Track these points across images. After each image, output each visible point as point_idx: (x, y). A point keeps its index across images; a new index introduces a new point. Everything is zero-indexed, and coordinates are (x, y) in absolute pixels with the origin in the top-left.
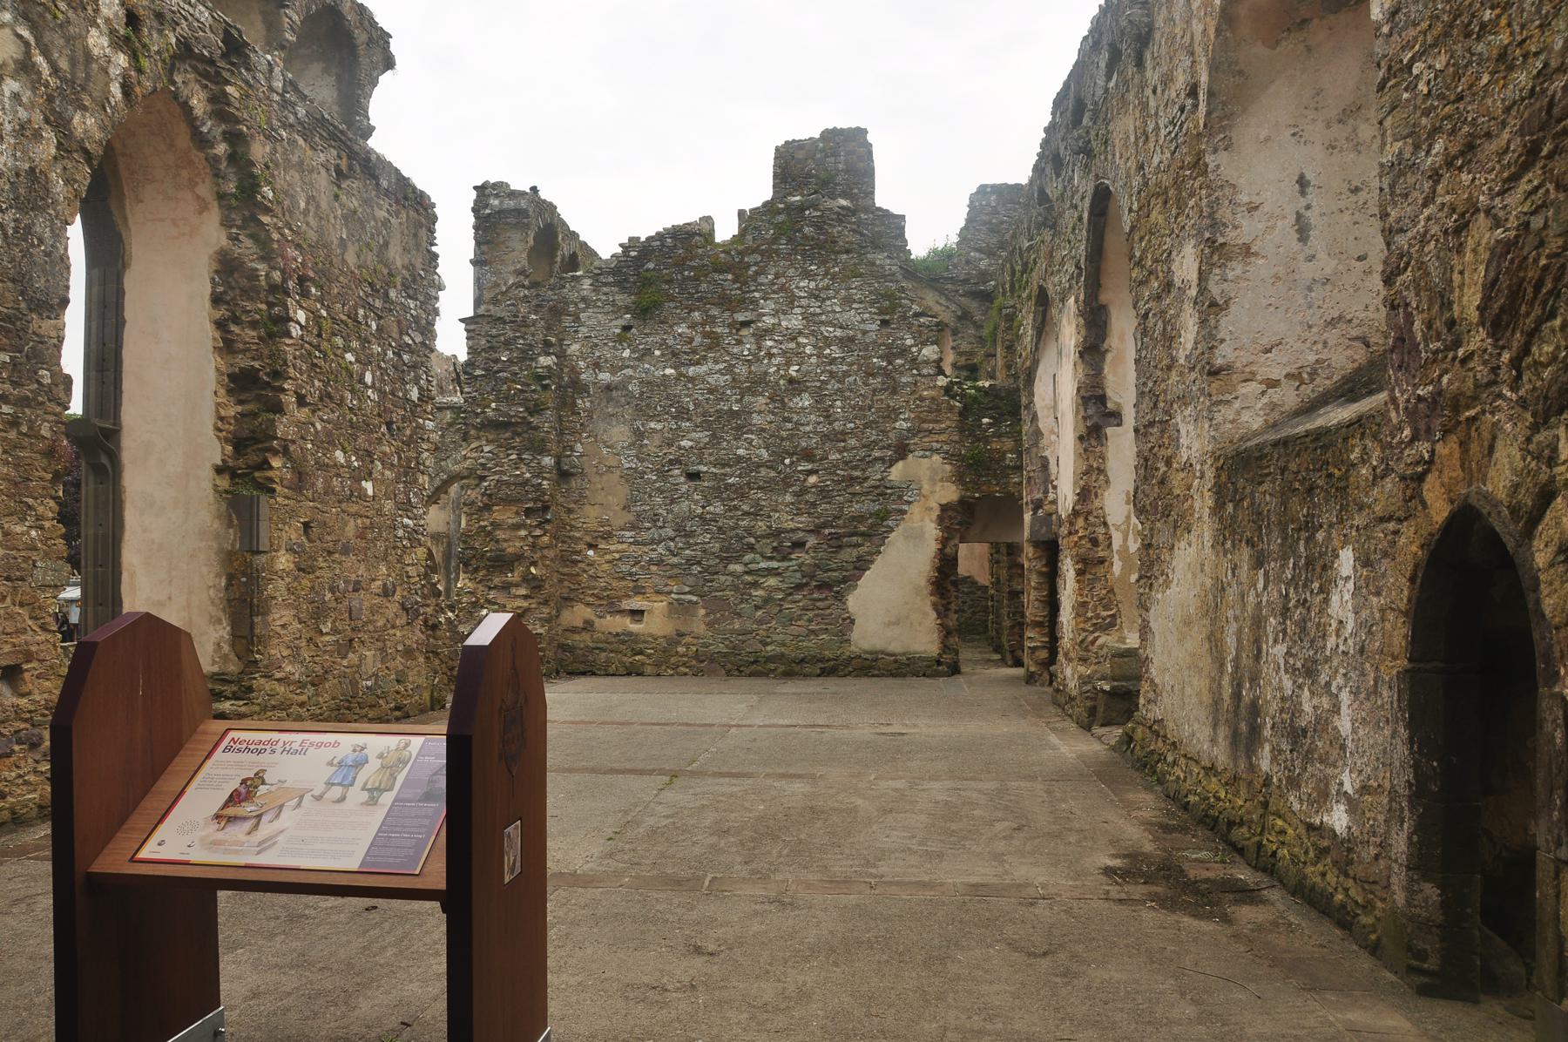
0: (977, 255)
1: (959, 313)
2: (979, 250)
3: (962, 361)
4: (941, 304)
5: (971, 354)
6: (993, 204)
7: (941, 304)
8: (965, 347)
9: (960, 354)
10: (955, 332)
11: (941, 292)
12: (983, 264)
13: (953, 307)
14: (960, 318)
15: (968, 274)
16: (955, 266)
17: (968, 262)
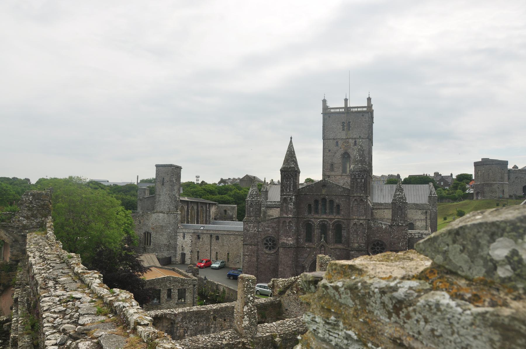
0: (23, 218)
1: (14, 240)
2: (24, 217)
3: (14, 258)
4: (7, 236)
5: (17, 256)
6: (31, 200)
7: (7, 236)
8: (15, 252)
9: (13, 255)
10: (12, 247)
11: (7, 231)
12: (24, 222)
13: (11, 237)
14: (14, 241)
15: (18, 225)
16: (13, 222)
17: (19, 221)
